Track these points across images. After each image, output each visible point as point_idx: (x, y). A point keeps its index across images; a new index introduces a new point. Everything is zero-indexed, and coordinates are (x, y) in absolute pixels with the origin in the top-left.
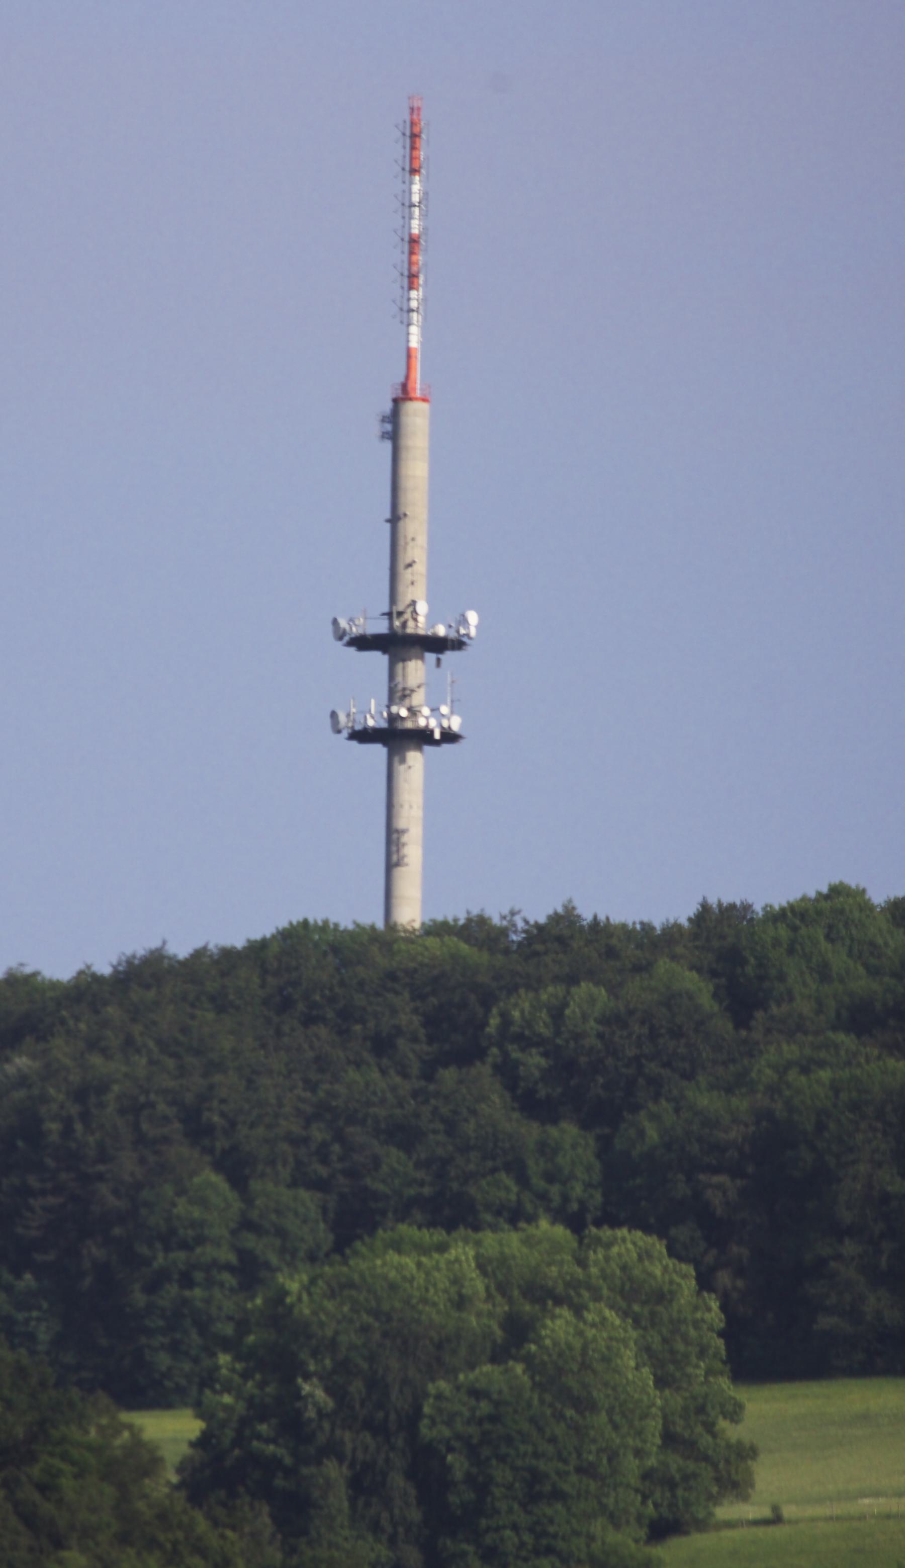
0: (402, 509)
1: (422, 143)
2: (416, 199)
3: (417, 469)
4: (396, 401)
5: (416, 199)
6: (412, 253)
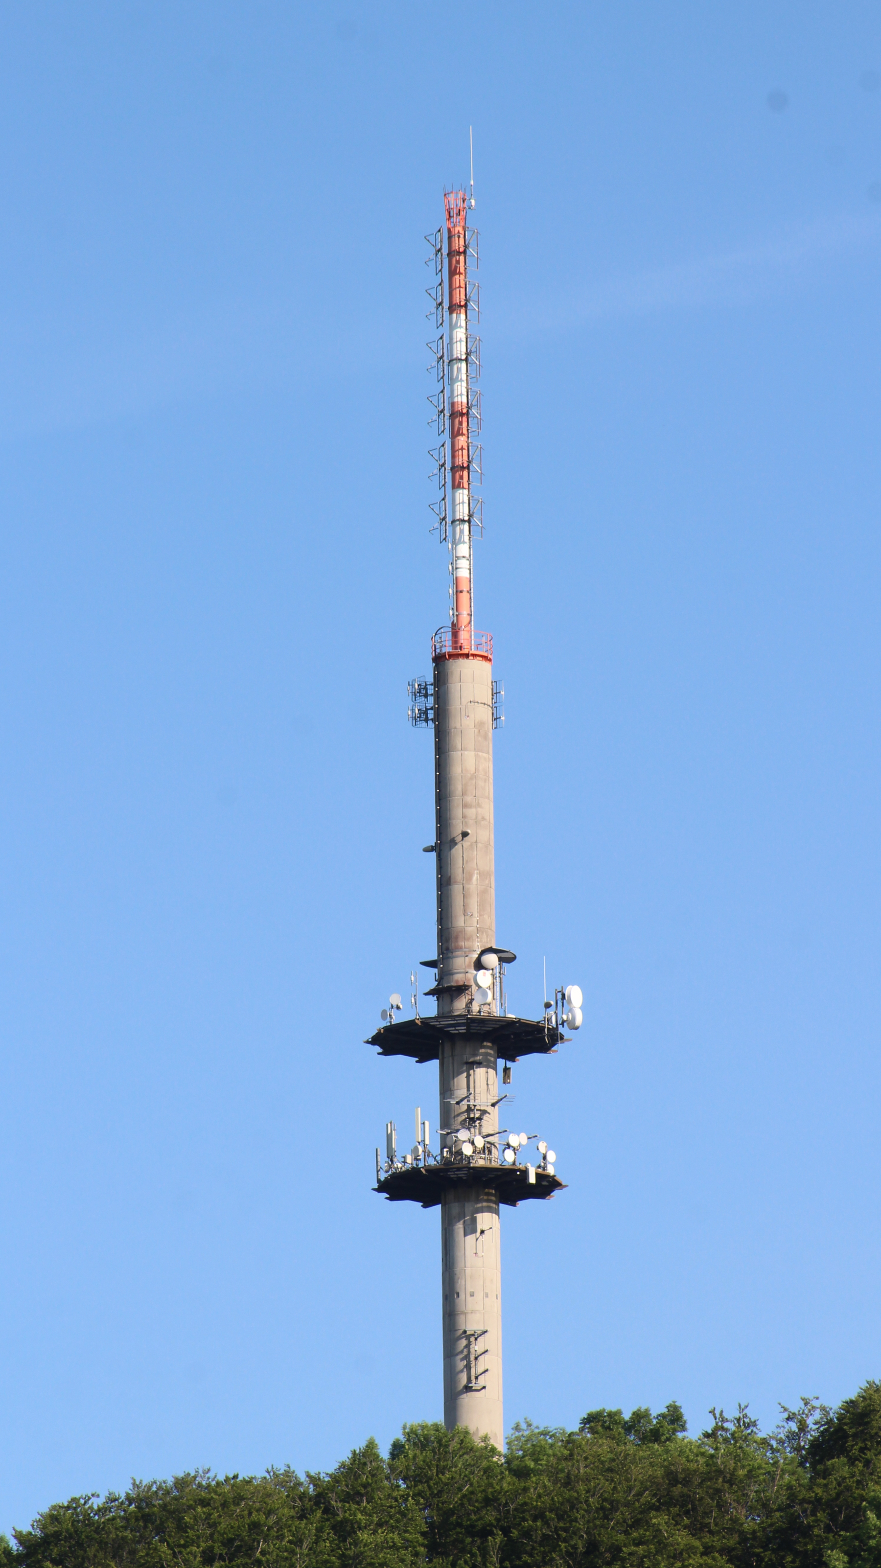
0: (456, 830)
1: (468, 265)
2: (460, 350)
3: (473, 761)
4: (440, 660)
5: (460, 350)
6: (455, 434)
